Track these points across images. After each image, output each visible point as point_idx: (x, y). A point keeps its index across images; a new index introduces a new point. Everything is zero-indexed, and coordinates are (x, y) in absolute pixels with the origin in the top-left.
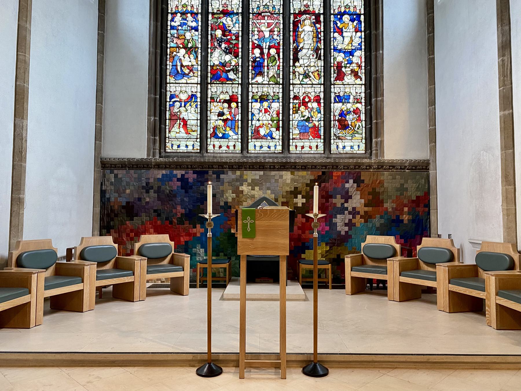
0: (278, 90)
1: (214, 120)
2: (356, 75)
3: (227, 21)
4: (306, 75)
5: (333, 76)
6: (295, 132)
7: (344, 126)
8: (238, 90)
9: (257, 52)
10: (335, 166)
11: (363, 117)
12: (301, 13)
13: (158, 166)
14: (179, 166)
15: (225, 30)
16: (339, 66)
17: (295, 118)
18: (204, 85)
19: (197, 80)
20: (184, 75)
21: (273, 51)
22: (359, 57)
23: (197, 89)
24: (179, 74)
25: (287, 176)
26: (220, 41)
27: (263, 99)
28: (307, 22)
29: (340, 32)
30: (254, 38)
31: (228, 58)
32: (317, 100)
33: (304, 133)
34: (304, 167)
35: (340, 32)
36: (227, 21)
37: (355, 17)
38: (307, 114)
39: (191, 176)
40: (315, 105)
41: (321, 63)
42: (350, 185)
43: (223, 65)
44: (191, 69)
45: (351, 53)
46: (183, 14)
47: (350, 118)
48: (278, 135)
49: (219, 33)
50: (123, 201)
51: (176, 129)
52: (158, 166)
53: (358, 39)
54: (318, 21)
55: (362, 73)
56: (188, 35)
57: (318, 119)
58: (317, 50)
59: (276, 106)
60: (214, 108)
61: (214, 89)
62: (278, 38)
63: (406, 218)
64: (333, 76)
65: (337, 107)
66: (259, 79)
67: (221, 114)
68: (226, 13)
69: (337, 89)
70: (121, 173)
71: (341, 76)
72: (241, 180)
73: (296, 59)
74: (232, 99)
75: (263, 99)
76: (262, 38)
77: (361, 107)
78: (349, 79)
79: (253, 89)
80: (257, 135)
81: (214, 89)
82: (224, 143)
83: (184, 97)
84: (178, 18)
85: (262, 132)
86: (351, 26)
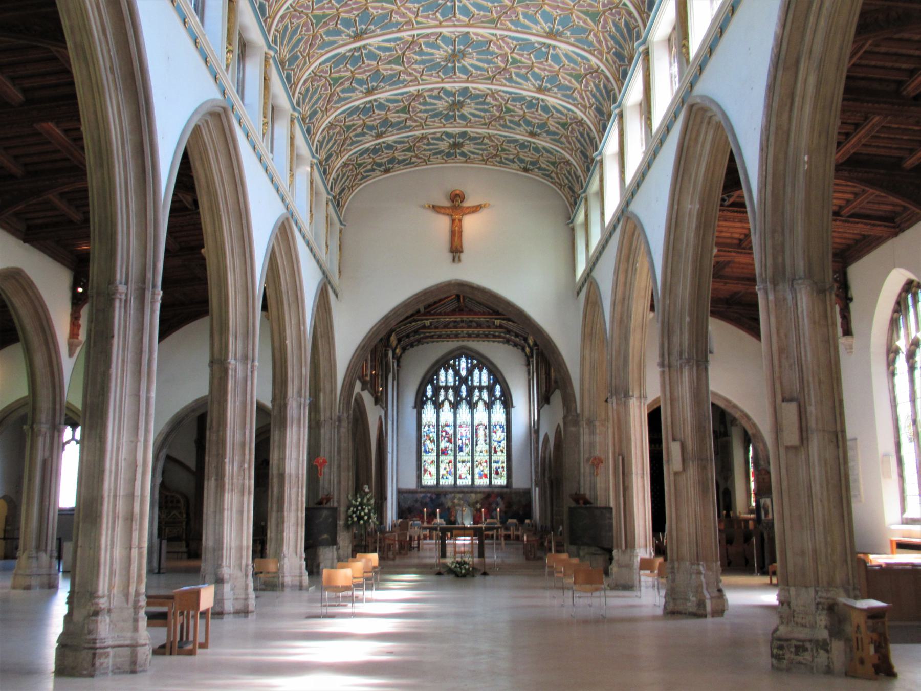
0: (469, 458)
1: (442, 472)
2: (502, 451)
3: (447, 428)
4: (481, 452)
5: (493, 452)
6: (476, 476)
7: (497, 473)
8: (452, 458)
9: (460, 442)
10: (493, 492)
11: (505, 469)
12: (478, 425)
13: (421, 492)
14: (429, 492)
15: (447, 433)
16: (495, 448)
17: (477, 470)
18: (438, 456)
19: (435, 454)
20: (429, 452)
21: (467, 442)
22: (504, 444)
23: (435, 458)
24: (427, 452)
25: (473, 495)
26: (444, 438)
27: (463, 462)
28: (482, 429)
29: (495, 433)
30: (459, 436)
31: (448, 444)
32: (486, 462)
33: (480, 477)
34: (480, 492)
35: (495, 433)
36: (447, 428)
37: (501, 426)
38: (482, 469)
39: (434, 497)
40: (485, 464)
41: (487, 447)
42: (499, 499)
43: (446, 448)
44: (432, 449)
45: (500, 442)
46: (429, 426)
47: (500, 470)
48: (469, 477)
49: (444, 434)
50: (407, 506)
51: (426, 475)
52: (421, 492)
53: (503, 435)
54: (486, 428)
55: (505, 451)
56: (431, 435)
57: (487, 471)
58: (485, 441)
59: (469, 465)
60: (442, 466)
61: (442, 458)
62: (469, 436)
63: (521, 513)
64: (493, 452)
65: (494, 465)
66: (461, 453)
67: (445, 469)
68: (447, 425)
69: (494, 458)
70: (406, 495)
71: (496, 452)
72: (454, 498)
73: (477, 445)
74: (450, 462)
75: (463, 462)
76: (462, 436)
77: (505, 465)
78: (499, 453)
79: (459, 458)
80: (460, 477)
81: (442, 458)
82: (447, 480)
83: (429, 461)
84: (427, 427)
85: (463, 476)
86: (500, 430)
